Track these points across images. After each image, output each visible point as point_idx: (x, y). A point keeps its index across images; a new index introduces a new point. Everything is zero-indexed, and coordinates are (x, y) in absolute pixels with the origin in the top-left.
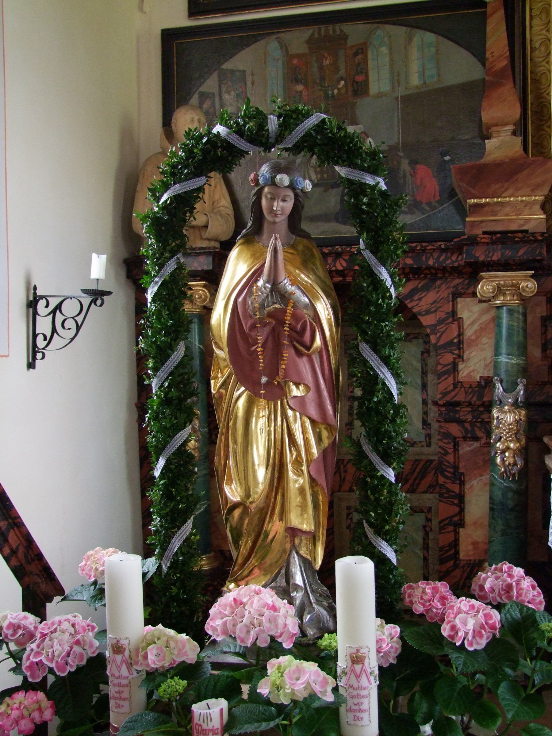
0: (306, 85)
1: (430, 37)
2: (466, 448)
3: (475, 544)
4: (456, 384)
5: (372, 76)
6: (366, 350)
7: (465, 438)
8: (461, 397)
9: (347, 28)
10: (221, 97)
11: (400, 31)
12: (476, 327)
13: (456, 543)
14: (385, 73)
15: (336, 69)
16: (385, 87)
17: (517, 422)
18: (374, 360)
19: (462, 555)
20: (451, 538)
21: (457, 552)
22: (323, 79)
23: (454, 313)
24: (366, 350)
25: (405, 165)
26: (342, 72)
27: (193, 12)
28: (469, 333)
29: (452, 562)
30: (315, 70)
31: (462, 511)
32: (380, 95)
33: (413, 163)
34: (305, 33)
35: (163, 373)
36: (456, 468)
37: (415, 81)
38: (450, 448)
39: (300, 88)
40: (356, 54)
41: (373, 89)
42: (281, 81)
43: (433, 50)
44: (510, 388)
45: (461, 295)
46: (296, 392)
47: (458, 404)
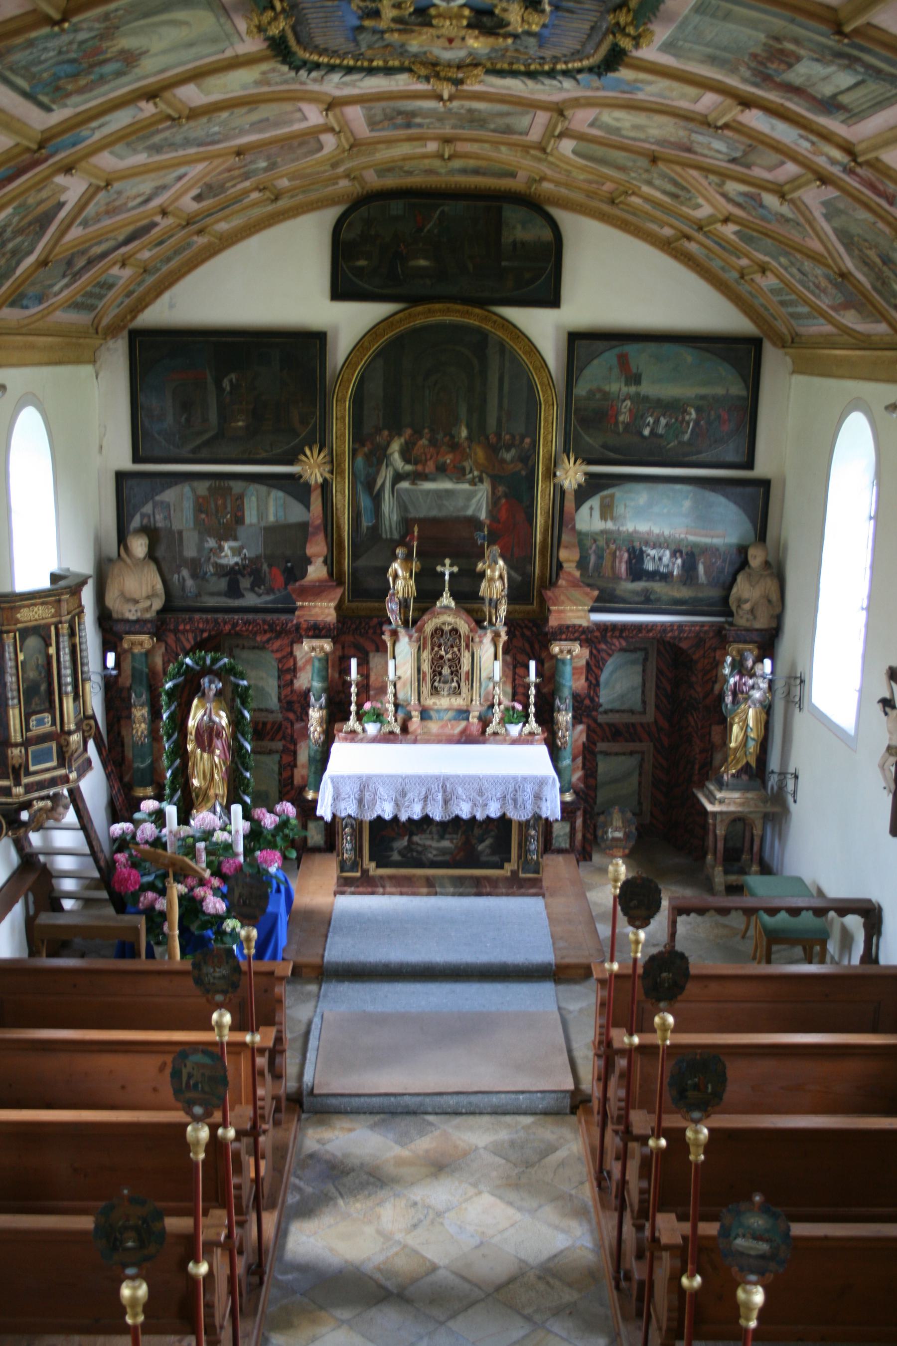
0: (207, 515)
1: (280, 494)
2: (298, 726)
3: (303, 777)
4: (292, 691)
5: (247, 513)
6: (240, 736)
7: (297, 720)
8: (295, 698)
9: (233, 484)
10: (154, 517)
11: (263, 489)
12: (304, 660)
13: (292, 777)
14: (254, 512)
15: (226, 508)
16: (254, 520)
17: (321, 718)
18: (242, 740)
19: (295, 782)
20: (289, 773)
21: (293, 781)
22: (217, 512)
23: (291, 653)
24: (240, 736)
25: (265, 567)
26: (229, 509)
27: (136, 459)
28: (300, 663)
29: (290, 787)
30: (213, 506)
31: (295, 759)
32: (251, 525)
33: (270, 566)
34: (206, 484)
35: (170, 742)
36: (292, 736)
37: (272, 518)
38: (289, 726)
39: (203, 516)
40: (237, 499)
41: (247, 521)
42: (191, 511)
43: (282, 501)
44: (318, 699)
45: (295, 642)
46: (218, 752)
47: (293, 702)
